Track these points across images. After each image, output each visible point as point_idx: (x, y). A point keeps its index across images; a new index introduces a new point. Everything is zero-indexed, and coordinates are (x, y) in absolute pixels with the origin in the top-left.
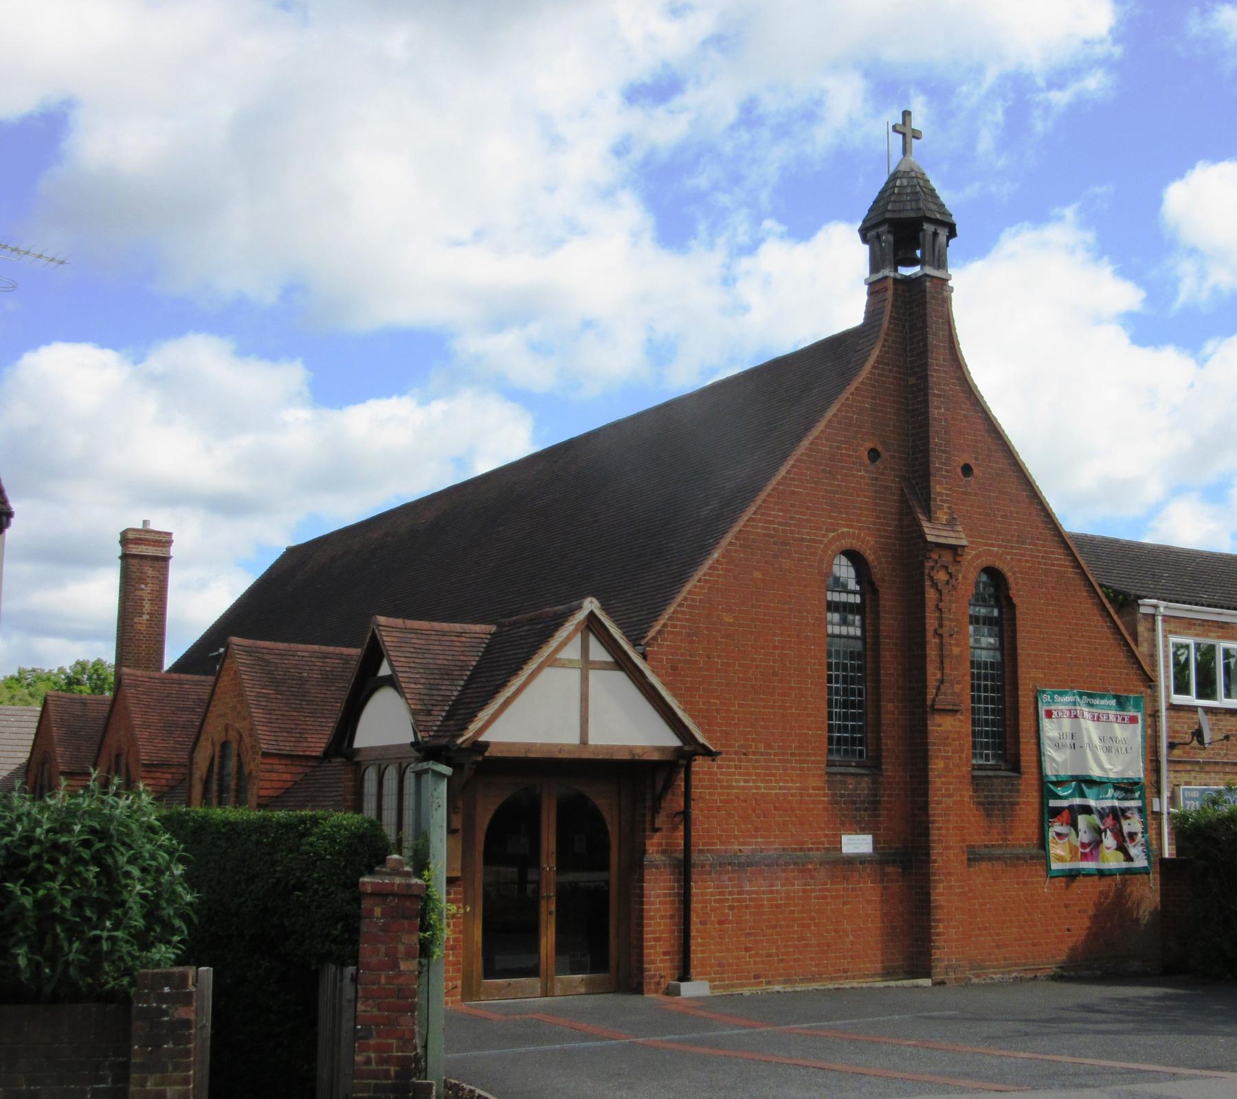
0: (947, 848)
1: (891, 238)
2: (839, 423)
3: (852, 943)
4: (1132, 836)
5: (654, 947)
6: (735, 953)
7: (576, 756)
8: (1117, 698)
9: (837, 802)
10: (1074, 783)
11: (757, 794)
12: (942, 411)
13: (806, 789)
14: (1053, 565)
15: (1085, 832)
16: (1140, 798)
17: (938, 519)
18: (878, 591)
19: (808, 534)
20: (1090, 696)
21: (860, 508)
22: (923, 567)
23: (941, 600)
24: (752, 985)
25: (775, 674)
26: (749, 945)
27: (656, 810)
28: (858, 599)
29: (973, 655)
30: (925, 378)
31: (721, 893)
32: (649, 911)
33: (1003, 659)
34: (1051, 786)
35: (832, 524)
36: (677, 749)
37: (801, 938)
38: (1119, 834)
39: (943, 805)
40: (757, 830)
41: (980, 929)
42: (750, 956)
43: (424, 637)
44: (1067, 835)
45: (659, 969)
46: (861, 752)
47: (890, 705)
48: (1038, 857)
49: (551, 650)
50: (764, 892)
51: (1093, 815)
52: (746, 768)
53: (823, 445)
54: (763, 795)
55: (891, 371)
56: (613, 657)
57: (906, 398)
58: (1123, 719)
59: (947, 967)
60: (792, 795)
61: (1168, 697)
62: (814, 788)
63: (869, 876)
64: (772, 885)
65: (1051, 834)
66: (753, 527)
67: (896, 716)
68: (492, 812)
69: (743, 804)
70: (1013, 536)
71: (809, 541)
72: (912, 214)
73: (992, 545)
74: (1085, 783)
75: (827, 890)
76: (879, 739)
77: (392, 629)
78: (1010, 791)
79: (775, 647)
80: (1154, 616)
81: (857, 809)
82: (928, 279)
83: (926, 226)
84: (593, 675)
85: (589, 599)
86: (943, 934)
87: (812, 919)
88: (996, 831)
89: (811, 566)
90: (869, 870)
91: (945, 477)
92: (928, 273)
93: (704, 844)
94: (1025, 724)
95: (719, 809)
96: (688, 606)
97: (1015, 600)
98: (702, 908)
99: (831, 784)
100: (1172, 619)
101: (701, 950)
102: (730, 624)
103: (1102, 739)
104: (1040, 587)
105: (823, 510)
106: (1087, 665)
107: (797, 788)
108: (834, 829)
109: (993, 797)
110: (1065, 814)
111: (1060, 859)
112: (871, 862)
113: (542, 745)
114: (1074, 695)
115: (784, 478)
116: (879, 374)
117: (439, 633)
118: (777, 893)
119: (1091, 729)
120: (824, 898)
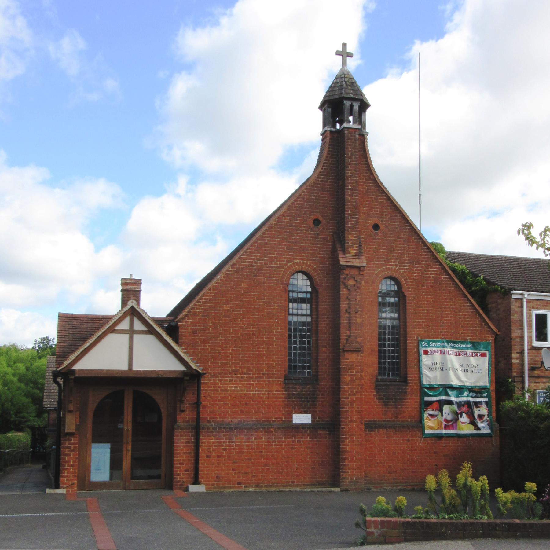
0: (351, 421)
1: (330, 110)
2: (295, 207)
3: (297, 468)
4: (481, 417)
5: (180, 468)
7: (126, 376)
8: (472, 343)
9: (290, 398)
10: (441, 389)
11: (242, 394)
13: (271, 391)
14: (431, 274)
15: (449, 414)
17: (349, 253)
19: (275, 264)
20: (454, 342)
21: (308, 250)
22: (340, 278)
23: (350, 295)
24: (236, 487)
25: (254, 334)
27: (181, 401)
30: (344, 181)
31: (218, 442)
32: (177, 450)
33: (400, 324)
34: (426, 390)
35: (290, 258)
36: (183, 371)
37: (265, 466)
38: (471, 415)
39: (350, 399)
40: (241, 411)
42: (235, 473)
43: (79, 321)
44: (436, 416)
45: (182, 478)
46: (309, 373)
47: (324, 349)
49: (109, 325)
50: (245, 442)
51: (453, 406)
52: (235, 381)
54: (245, 394)
55: (328, 179)
56: (147, 328)
58: (477, 355)
59: (350, 482)
60: (263, 394)
61: (530, 342)
62: (276, 391)
64: (249, 439)
65: (426, 415)
66: (242, 262)
69: (234, 399)
70: (405, 260)
71: (277, 267)
72: (337, 97)
74: (447, 388)
75: (282, 442)
76: (317, 366)
77: (63, 318)
80: (522, 299)
81: (303, 401)
82: (346, 129)
83: (345, 102)
84: (135, 336)
85: (131, 301)
87: (273, 456)
90: (308, 432)
91: (354, 231)
94: (411, 357)
95: (219, 401)
96: (203, 302)
97: (406, 293)
100: (535, 301)
101: (206, 470)
102: (228, 310)
103: (462, 365)
104: (424, 286)
105: (285, 252)
106: (454, 326)
107: (266, 391)
108: (287, 411)
109: (389, 395)
110: (435, 405)
111: (431, 428)
112: (309, 428)
114: (443, 342)
115: (261, 236)
116: (321, 181)
117: (89, 319)
119: (453, 360)
120: (280, 445)
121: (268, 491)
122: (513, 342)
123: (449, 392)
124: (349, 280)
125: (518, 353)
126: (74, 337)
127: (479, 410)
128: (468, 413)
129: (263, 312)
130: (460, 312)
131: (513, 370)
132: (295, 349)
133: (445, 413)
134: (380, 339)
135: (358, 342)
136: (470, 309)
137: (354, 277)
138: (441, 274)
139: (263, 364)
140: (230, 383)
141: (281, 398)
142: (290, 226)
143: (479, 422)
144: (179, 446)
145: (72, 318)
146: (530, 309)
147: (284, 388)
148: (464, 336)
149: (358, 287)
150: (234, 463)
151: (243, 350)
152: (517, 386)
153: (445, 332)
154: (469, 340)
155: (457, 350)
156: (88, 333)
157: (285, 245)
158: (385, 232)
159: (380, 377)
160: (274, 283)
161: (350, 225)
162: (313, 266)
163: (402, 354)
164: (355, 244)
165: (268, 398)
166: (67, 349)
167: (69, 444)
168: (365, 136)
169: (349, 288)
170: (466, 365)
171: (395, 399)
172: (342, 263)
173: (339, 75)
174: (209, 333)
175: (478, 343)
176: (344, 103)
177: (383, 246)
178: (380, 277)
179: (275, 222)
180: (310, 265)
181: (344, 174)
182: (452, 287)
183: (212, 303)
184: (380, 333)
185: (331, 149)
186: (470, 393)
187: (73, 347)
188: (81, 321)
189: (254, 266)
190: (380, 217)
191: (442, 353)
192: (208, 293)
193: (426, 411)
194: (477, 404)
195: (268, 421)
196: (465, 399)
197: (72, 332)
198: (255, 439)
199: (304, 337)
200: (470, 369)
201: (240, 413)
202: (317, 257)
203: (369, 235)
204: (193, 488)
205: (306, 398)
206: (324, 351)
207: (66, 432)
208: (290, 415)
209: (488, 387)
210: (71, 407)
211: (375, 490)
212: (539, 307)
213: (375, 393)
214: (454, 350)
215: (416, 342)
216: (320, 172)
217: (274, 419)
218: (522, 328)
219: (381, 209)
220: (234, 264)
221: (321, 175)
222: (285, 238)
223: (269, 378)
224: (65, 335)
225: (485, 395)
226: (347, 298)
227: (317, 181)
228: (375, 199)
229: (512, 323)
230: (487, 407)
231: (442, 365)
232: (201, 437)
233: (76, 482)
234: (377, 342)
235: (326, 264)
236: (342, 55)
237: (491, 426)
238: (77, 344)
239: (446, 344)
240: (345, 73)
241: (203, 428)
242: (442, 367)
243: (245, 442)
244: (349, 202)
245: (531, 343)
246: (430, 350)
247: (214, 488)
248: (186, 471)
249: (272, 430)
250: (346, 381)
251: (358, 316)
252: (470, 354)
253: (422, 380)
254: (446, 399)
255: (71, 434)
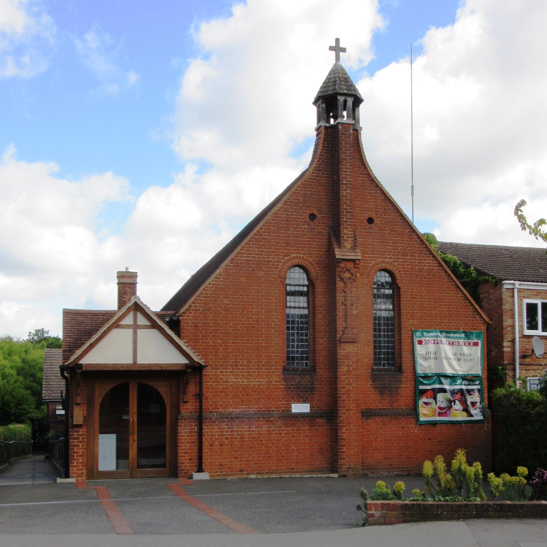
0: (348, 410)
3: (297, 456)
4: (473, 404)
5: (184, 456)
6: (229, 460)
8: (465, 333)
9: (289, 388)
10: (435, 378)
12: (348, 191)
13: (271, 382)
14: (425, 266)
16: (479, 384)
17: (345, 246)
18: (314, 284)
19: (272, 258)
20: (446, 332)
21: (304, 244)
22: (335, 272)
23: (346, 287)
24: (238, 474)
26: (236, 456)
27: (184, 393)
28: (305, 289)
29: (376, 314)
30: (338, 176)
31: (221, 432)
32: (181, 440)
34: (421, 379)
35: (287, 253)
36: (186, 364)
37: (266, 454)
38: (464, 402)
39: (346, 389)
40: (242, 402)
41: (374, 450)
42: (237, 461)
43: (84, 317)
44: (430, 403)
45: (187, 467)
47: (321, 341)
48: (412, 415)
50: (246, 431)
51: (446, 393)
52: (236, 372)
53: (282, 214)
54: (246, 385)
55: (323, 174)
57: (333, 187)
58: (469, 344)
59: (347, 468)
60: (263, 385)
61: (521, 331)
62: (276, 382)
63: (307, 423)
64: (250, 428)
65: (421, 402)
66: (241, 257)
67: (325, 346)
68: (104, 395)
69: (235, 390)
70: (399, 252)
71: (274, 262)
73: (386, 258)
74: (441, 376)
76: (315, 357)
77: (69, 314)
78: (395, 381)
79: (253, 314)
80: (513, 289)
81: (301, 391)
82: (340, 125)
84: (139, 331)
86: (346, 452)
87: (273, 444)
88: (386, 401)
89: (274, 274)
90: (307, 421)
91: (349, 225)
92: (339, 121)
93: (212, 409)
94: (405, 348)
95: (221, 392)
96: (203, 297)
97: (400, 285)
98: (210, 438)
99: (286, 380)
101: (210, 458)
102: (228, 304)
103: (455, 354)
104: (417, 277)
105: (282, 246)
106: (447, 317)
107: (266, 382)
108: (287, 401)
109: (384, 384)
111: (425, 415)
112: (307, 417)
113: (113, 365)
114: (437, 332)
115: (258, 231)
116: (316, 176)
118: (253, 432)
119: (447, 350)
120: (280, 434)
121: (269, 478)
122: (504, 332)
123: (443, 379)
124: (344, 273)
125: (509, 341)
126: (79, 332)
127: (472, 398)
128: (461, 400)
129: (262, 305)
130: (452, 302)
131: (505, 359)
132: (293, 340)
133: (439, 401)
134: (375, 330)
135: (354, 333)
136: (462, 299)
137: (350, 270)
138: (435, 266)
139: (262, 356)
140: (231, 374)
141: (281, 388)
142: (286, 221)
143: (471, 409)
144: (183, 436)
145: (77, 313)
146: (521, 298)
147: (283, 378)
148: (457, 326)
149: (353, 280)
150: (236, 451)
151: (242, 343)
152: (509, 374)
153: (438, 322)
154: (461, 330)
155: (450, 340)
156: (93, 328)
157: (282, 240)
158: (379, 226)
159: (375, 367)
160: (272, 277)
161: (345, 220)
162: (309, 260)
163: (396, 344)
164: (351, 237)
165: (268, 388)
166: (73, 344)
167: (77, 435)
168: (359, 131)
169: (344, 281)
170: (459, 354)
171: (390, 388)
172: (337, 257)
174: (210, 326)
175: (471, 332)
176: (338, 98)
177: (378, 239)
178: (375, 270)
179: (272, 217)
180: (306, 259)
181: (339, 169)
182: (445, 279)
183: (213, 297)
184: (375, 324)
185: (325, 145)
186: (463, 381)
187: (79, 342)
188: (85, 317)
189: (252, 261)
190: (375, 211)
191: (436, 343)
192: (208, 287)
193: (421, 399)
194: (469, 392)
195: (268, 411)
196: (458, 387)
197: (76, 328)
198: (256, 428)
199: (302, 329)
200: (463, 358)
201: (241, 403)
202: (313, 251)
203: (364, 229)
204: (197, 476)
205: (305, 388)
206: (322, 342)
207: (74, 424)
208: (289, 404)
209: (480, 375)
210: (79, 400)
211: (372, 475)
212: (530, 296)
213: (371, 383)
214: (449, 340)
215: (410, 332)
216: (315, 167)
217: (273, 409)
218: (513, 317)
219: (376, 202)
220: (233, 259)
221: (316, 170)
222: (282, 233)
223: (268, 369)
224: (70, 331)
225: (477, 383)
226: (343, 290)
227: (313, 176)
228: (369, 193)
229: (503, 313)
230: (480, 394)
231: (436, 354)
232: (204, 427)
233: (85, 471)
234: (372, 333)
235: (322, 258)
237: (483, 412)
238: (82, 339)
239: (439, 334)
241: (206, 419)
242: (435, 356)
243: (246, 431)
244: (344, 196)
245: (522, 331)
246: (424, 340)
247: (218, 475)
248: (190, 460)
249: (272, 419)
250: (343, 372)
251: (353, 308)
252: (462, 343)
253: (416, 369)
254: (440, 387)
255: (79, 426)
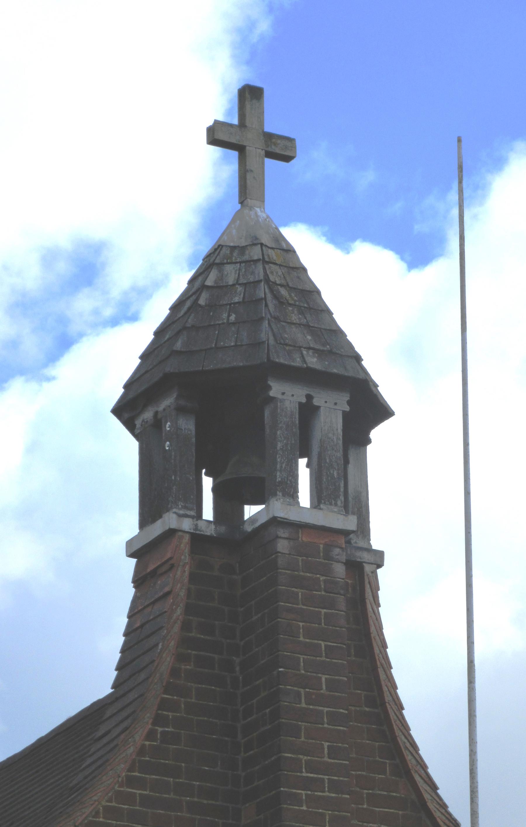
82: (282, 533)
168: (368, 568)
173: (233, 248)
176: (272, 393)
216: (141, 751)
236: (240, 149)
240: (265, 240)
